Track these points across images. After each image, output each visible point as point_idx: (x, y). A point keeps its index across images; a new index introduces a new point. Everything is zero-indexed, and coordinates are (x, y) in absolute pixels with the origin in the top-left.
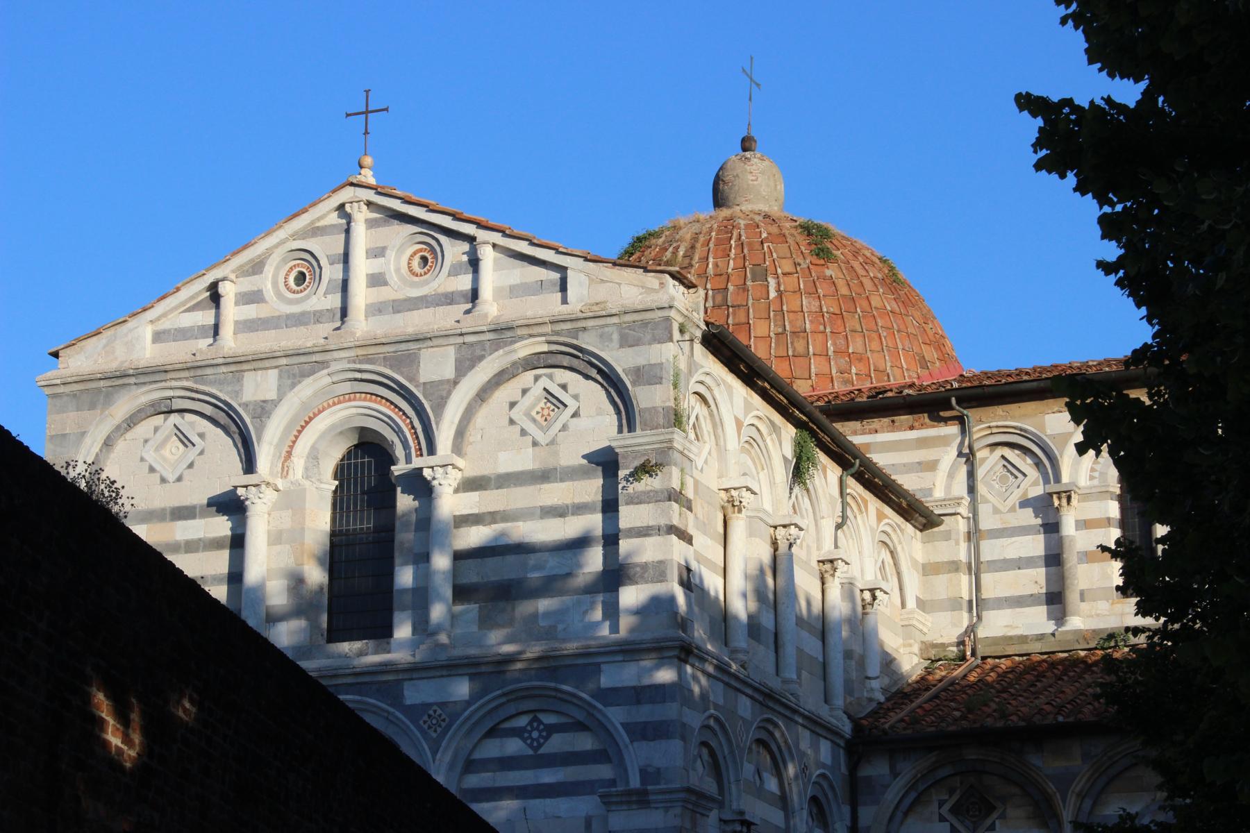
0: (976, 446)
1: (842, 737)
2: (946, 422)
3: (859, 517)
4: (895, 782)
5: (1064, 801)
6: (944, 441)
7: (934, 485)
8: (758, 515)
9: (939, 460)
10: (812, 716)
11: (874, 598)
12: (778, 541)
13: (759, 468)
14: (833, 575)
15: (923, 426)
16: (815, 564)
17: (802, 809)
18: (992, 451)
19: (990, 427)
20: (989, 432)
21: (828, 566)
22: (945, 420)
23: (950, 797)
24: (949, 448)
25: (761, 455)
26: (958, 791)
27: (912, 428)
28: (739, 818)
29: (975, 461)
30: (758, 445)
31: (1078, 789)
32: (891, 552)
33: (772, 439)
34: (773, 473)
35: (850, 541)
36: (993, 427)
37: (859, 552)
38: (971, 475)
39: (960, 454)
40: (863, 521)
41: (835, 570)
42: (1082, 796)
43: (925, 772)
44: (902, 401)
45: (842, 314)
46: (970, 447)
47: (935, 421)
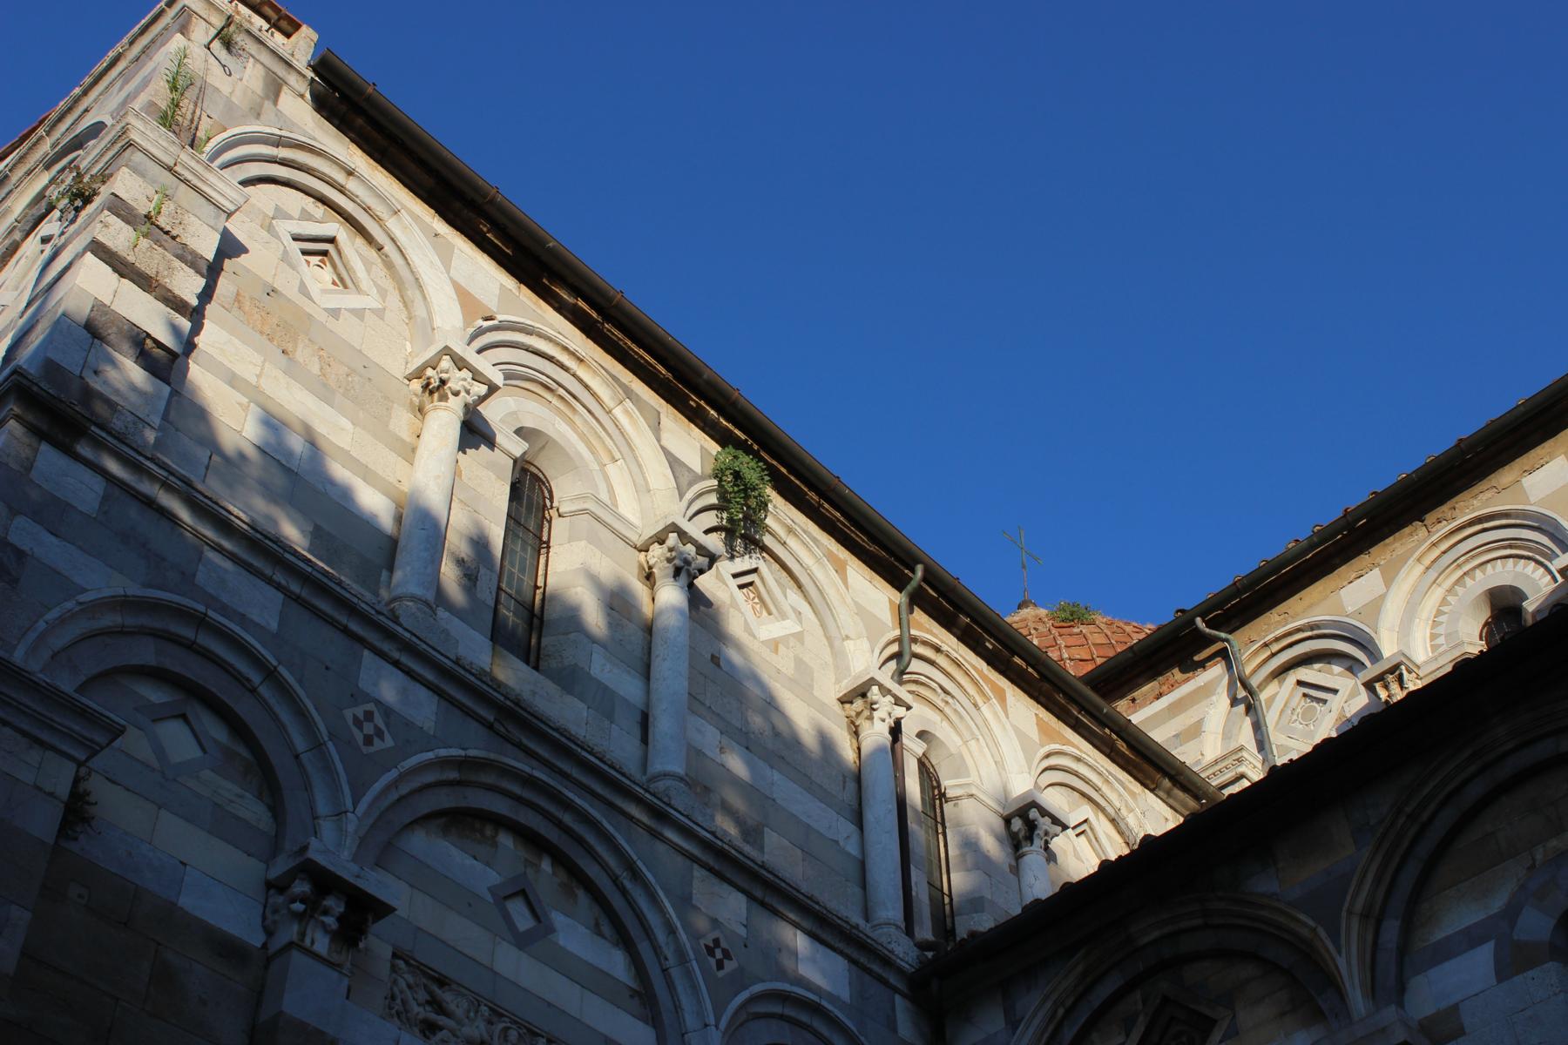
0: (1254, 682)
1: (887, 962)
2: (1204, 667)
3: (984, 708)
4: (1015, 1037)
5: (1335, 936)
6: (1206, 691)
7: (1202, 755)
8: (586, 506)
9: (1202, 719)
10: (726, 847)
11: (1031, 826)
12: (654, 570)
13: (605, 459)
14: (870, 718)
15: (1173, 687)
16: (837, 706)
17: (706, 1025)
18: (1281, 683)
19: (1266, 645)
20: (1269, 653)
21: (859, 704)
22: (1202, 665)
23: (1128, 1036)
24: (1214, 698)
25: (603, 434)
26: (1141, 1018)
27: (1159, 696)
28: (299, 860)
29: (1257, 703)
30: (589, 411)
31: (1359, 906)
32: (1113, 821)
33: (626, 411)
34: (643, 473)
35: (973, 743)
36: (1271, 643)
37: (996, 762)
38: (1258, 727)
39: (1234, 702)
40: (995, 714)
41: (872, 707)
42: (1374, 918)
43: (1069, 1002)
44: (1130, 655)
45: (1093, 659)
46: (1245, 686)
47: (1188, 672)
